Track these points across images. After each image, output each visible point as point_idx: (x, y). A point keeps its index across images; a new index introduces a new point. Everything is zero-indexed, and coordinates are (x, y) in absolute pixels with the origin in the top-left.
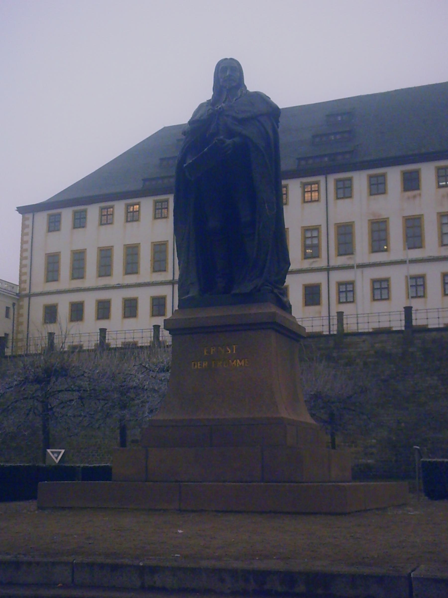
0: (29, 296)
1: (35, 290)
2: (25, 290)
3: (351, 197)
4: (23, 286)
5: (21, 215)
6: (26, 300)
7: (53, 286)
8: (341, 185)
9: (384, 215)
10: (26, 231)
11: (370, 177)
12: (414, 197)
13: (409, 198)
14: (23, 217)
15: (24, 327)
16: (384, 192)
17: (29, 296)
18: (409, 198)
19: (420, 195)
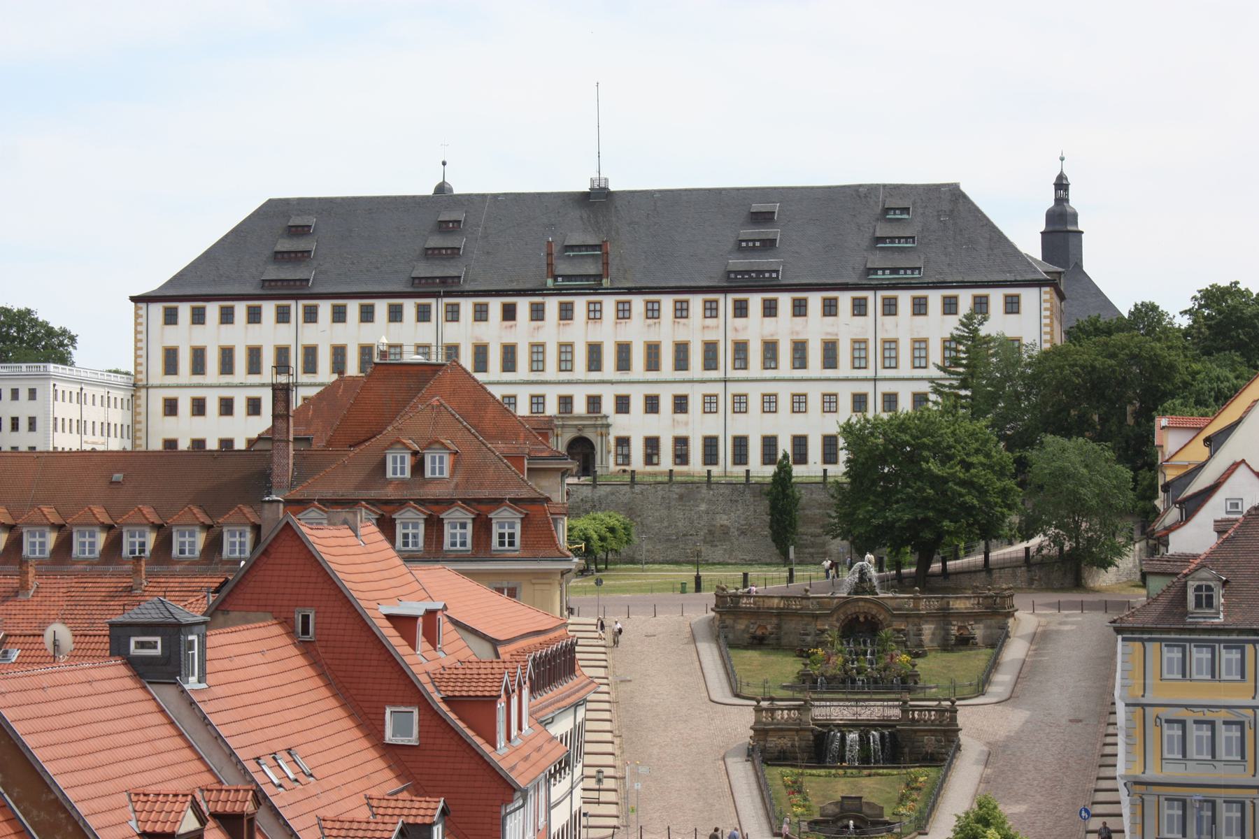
0: (147, 387)
1: (152, 382)
2: (141, 380)
3: (457, 321)
4: (139, 376)
5: (133, 304)
6: (143, 391)
7: (171, 380)
8: (450, 308)
9: (485, 340)
10: (140, 320)
11: (476, 305)
12: (511, 327)
13: (506, 327)
14: (136, 306)
15: (142, 418)
16: (486, 320)
17: (147, 387)
18: (506, 327)
19: (516, 325)
